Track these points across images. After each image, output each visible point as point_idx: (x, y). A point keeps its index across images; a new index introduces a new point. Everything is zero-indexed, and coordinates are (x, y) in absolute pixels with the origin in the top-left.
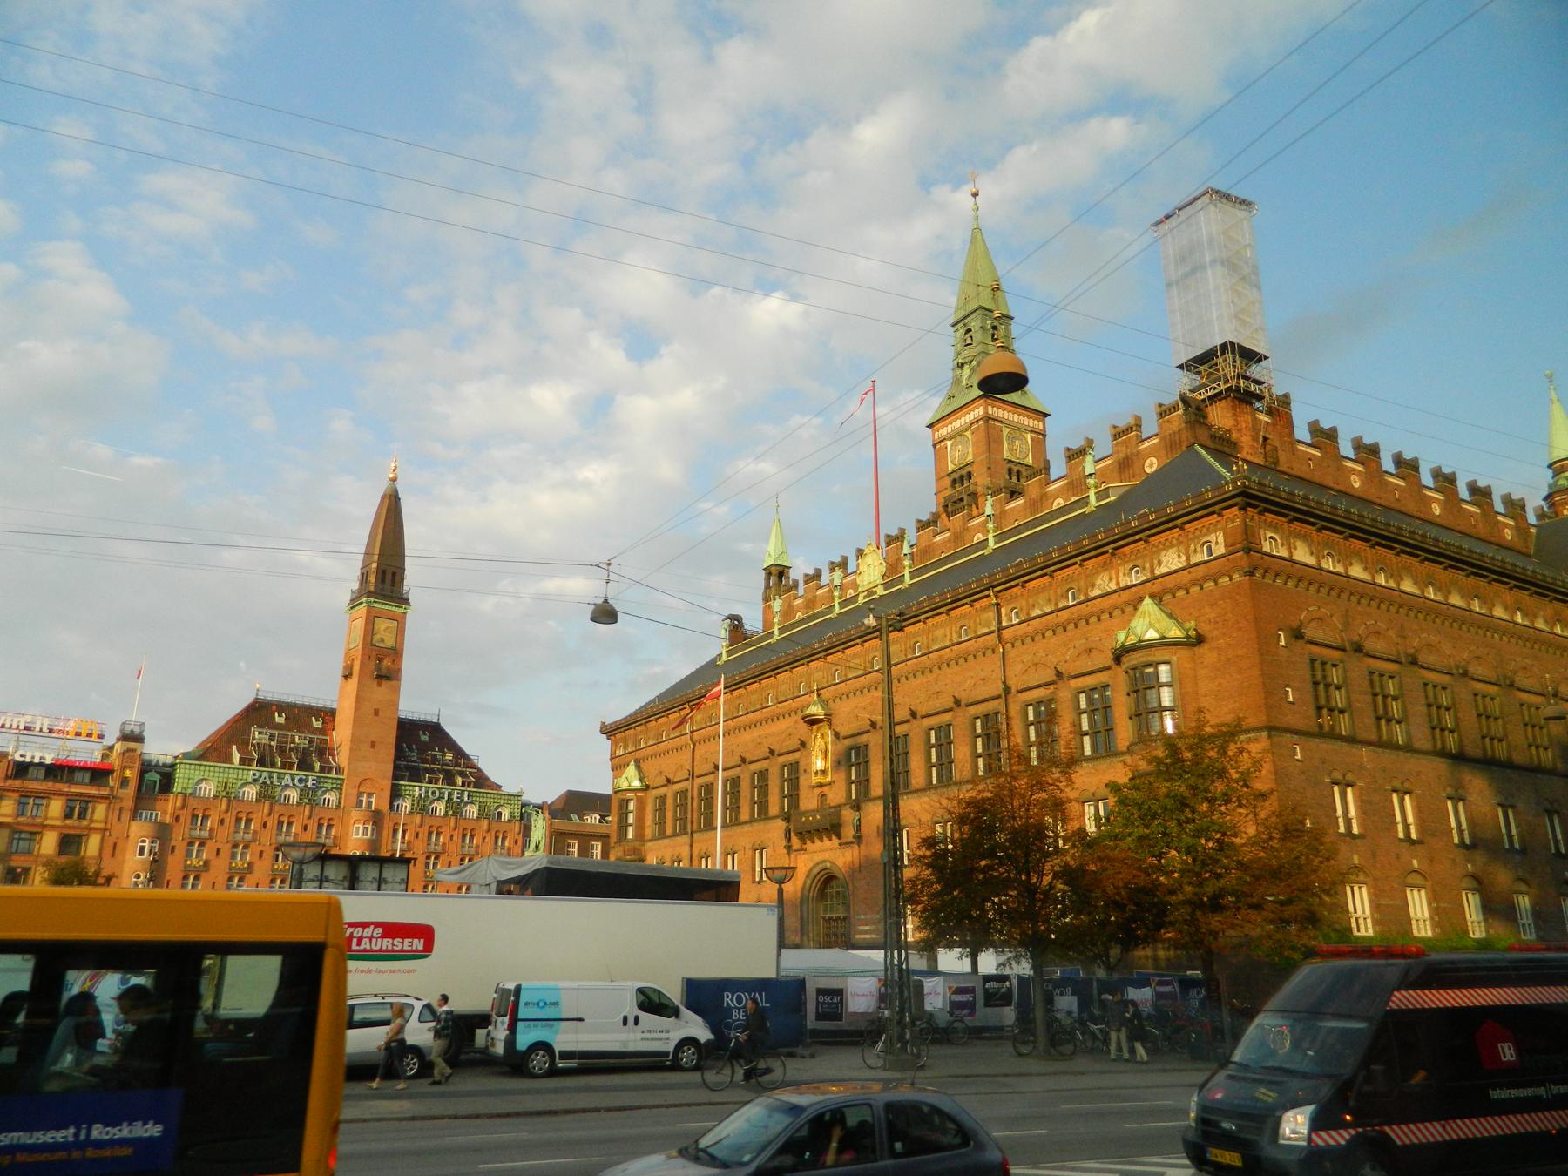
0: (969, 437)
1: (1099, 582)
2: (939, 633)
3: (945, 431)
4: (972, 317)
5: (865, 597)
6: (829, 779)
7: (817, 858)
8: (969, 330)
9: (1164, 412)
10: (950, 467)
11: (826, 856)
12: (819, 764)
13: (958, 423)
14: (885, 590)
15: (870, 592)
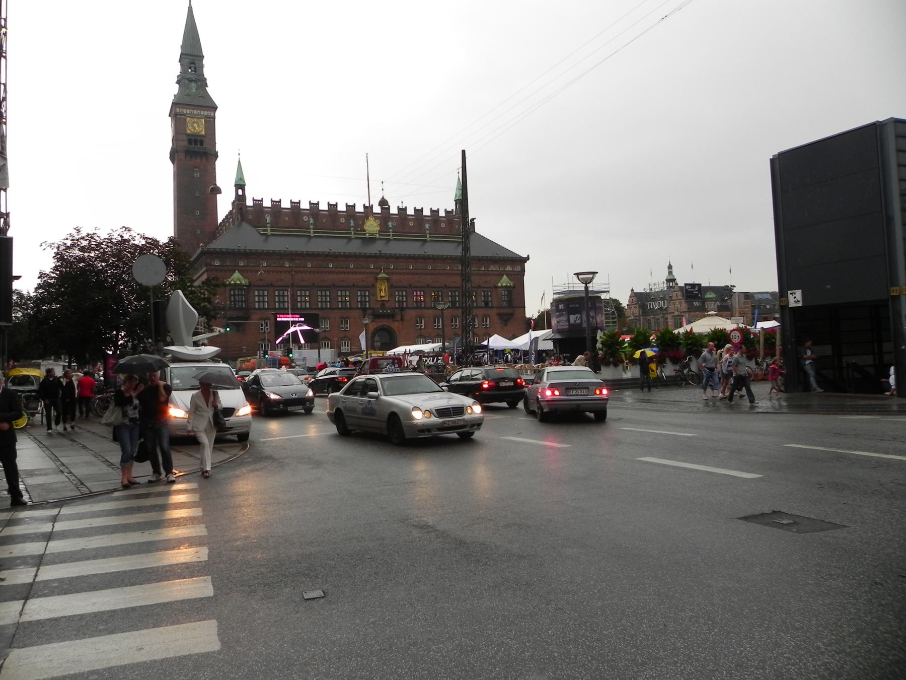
0: (203, 122)
1: (491, 267)
2: (439, 265)
3: (185, 111)
4: (196, 58)
5: (369, 235)
6: (387, 299)
7: (380, 324)
8: (195, 64)
9: (447, 212)
10: (188, 132)
11: (385, 323)
12: (382, 294)
13: (195, 112)
14: (379, 236)
15: (372, 235)
